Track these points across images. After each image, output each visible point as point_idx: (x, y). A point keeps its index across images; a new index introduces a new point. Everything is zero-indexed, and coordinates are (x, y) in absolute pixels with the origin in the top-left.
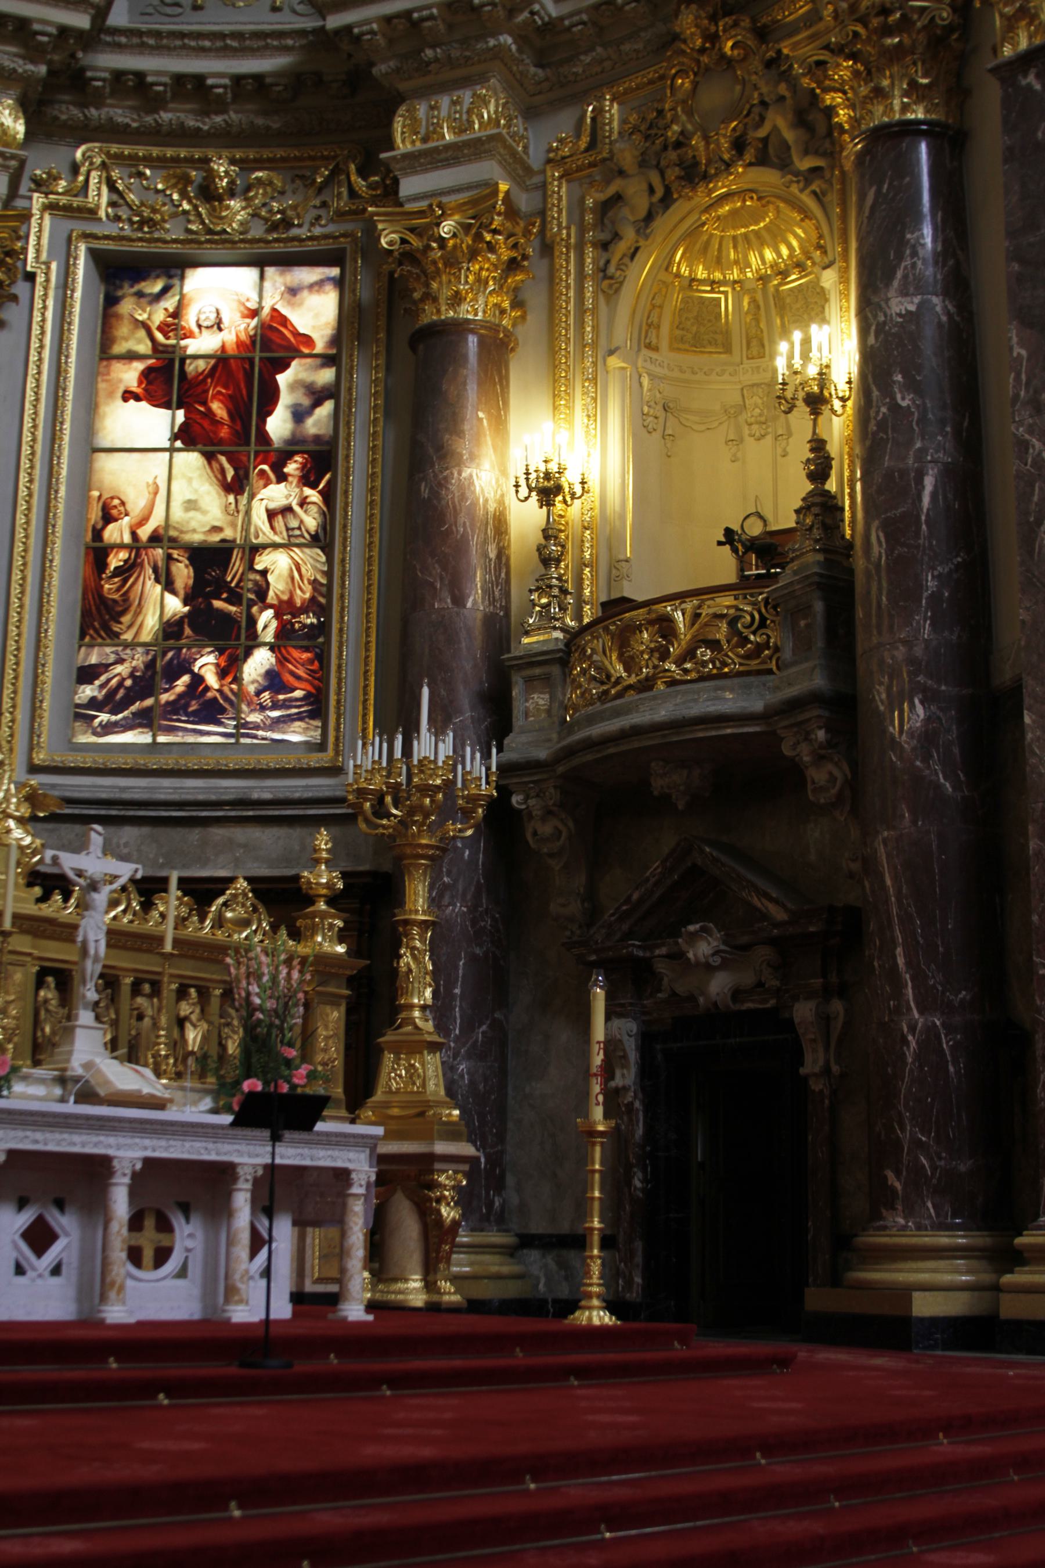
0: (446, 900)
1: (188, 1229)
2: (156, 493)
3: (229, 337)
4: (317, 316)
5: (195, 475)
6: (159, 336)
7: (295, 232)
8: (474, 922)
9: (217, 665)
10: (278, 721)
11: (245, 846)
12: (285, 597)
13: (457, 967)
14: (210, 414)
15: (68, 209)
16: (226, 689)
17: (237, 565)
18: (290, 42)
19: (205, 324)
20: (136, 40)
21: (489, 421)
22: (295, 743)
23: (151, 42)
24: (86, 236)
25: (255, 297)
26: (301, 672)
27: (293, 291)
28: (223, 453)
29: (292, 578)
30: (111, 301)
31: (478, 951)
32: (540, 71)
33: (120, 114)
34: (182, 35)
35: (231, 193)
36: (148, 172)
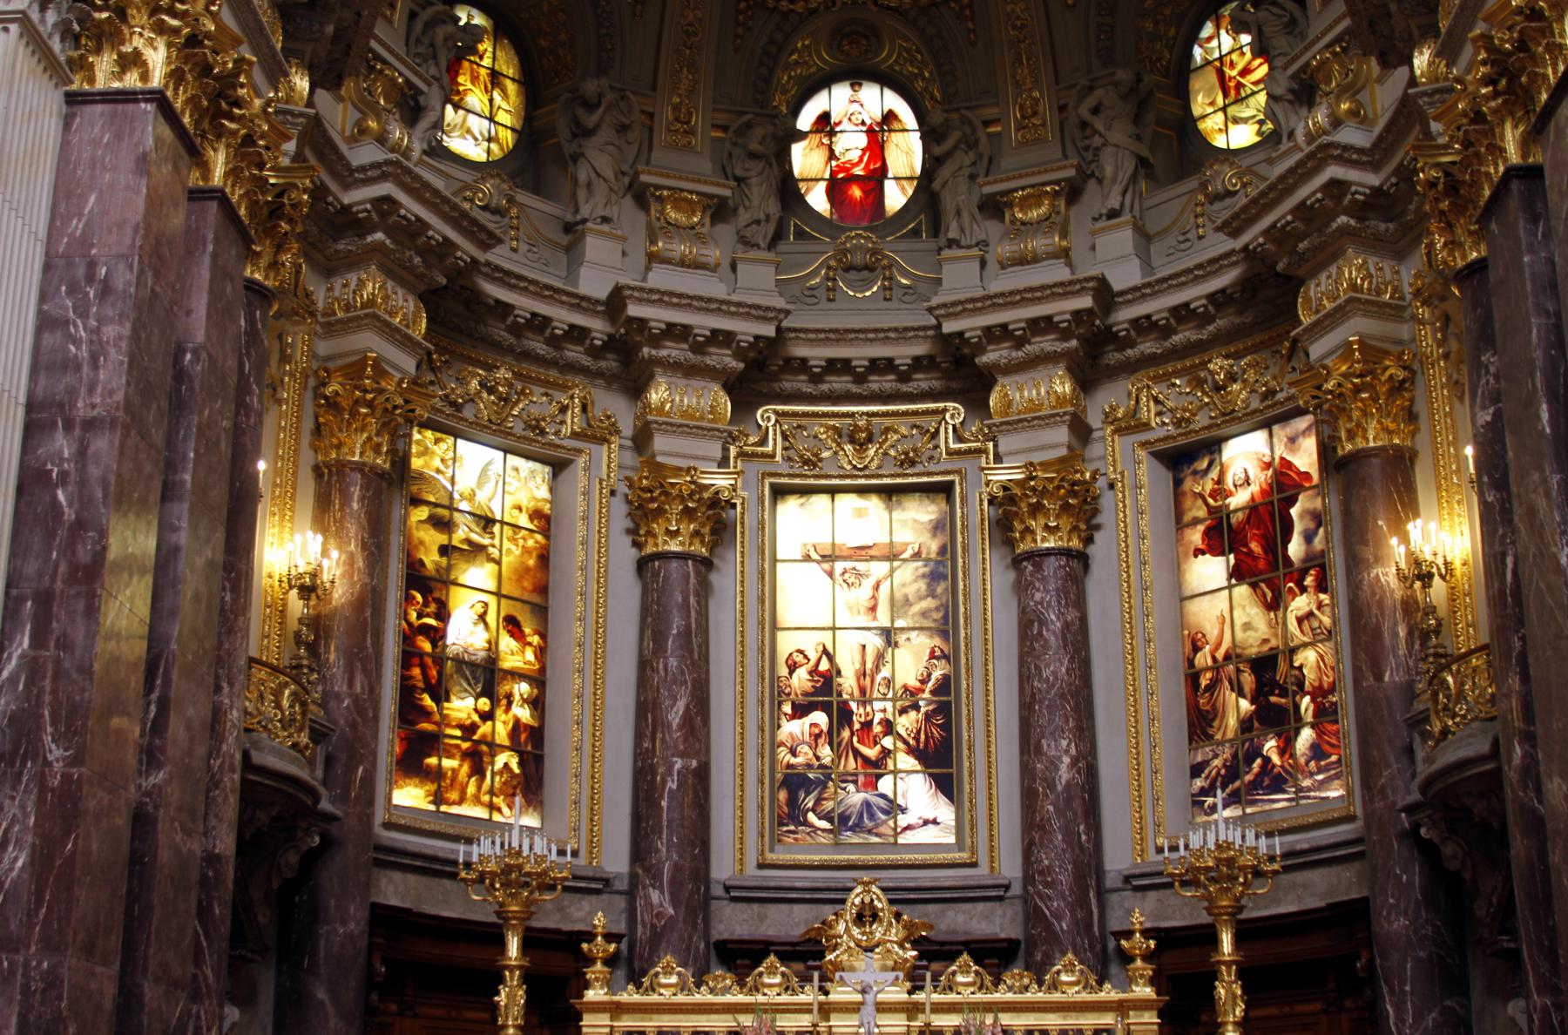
0: (1393, 917)
2: (1223, 623)
3: (1255, 488)
4: (1310, 455)
5: (1246, 602)
6: (1211, 501)
7: (1280, 396)
9: (1278, 747)
10: (1322, 782)
11: (1303, 886)
12: (1316, 684)
13: (1405, 969)
14: (1250, 549)
15: (1127, 428)
17: (1282, 666)
18: (1234, 259)
19: (1239, 483)
20: (1138, 294)
21: (1388, 527)
22: (1334, 798)
23: (1148, 291)
24: (1144, 444)
25: (1268, 452)
26: (1333, 741)
27: (1292, 440)
28: (1263, 581)
29: (1319, 667)
30: (1178, 483)
31: (1422, 954)
32: (1391, 225)
33: (1148, 347)
34: (1164, 280)
35: (1232, 378)
36: (1178, 382)
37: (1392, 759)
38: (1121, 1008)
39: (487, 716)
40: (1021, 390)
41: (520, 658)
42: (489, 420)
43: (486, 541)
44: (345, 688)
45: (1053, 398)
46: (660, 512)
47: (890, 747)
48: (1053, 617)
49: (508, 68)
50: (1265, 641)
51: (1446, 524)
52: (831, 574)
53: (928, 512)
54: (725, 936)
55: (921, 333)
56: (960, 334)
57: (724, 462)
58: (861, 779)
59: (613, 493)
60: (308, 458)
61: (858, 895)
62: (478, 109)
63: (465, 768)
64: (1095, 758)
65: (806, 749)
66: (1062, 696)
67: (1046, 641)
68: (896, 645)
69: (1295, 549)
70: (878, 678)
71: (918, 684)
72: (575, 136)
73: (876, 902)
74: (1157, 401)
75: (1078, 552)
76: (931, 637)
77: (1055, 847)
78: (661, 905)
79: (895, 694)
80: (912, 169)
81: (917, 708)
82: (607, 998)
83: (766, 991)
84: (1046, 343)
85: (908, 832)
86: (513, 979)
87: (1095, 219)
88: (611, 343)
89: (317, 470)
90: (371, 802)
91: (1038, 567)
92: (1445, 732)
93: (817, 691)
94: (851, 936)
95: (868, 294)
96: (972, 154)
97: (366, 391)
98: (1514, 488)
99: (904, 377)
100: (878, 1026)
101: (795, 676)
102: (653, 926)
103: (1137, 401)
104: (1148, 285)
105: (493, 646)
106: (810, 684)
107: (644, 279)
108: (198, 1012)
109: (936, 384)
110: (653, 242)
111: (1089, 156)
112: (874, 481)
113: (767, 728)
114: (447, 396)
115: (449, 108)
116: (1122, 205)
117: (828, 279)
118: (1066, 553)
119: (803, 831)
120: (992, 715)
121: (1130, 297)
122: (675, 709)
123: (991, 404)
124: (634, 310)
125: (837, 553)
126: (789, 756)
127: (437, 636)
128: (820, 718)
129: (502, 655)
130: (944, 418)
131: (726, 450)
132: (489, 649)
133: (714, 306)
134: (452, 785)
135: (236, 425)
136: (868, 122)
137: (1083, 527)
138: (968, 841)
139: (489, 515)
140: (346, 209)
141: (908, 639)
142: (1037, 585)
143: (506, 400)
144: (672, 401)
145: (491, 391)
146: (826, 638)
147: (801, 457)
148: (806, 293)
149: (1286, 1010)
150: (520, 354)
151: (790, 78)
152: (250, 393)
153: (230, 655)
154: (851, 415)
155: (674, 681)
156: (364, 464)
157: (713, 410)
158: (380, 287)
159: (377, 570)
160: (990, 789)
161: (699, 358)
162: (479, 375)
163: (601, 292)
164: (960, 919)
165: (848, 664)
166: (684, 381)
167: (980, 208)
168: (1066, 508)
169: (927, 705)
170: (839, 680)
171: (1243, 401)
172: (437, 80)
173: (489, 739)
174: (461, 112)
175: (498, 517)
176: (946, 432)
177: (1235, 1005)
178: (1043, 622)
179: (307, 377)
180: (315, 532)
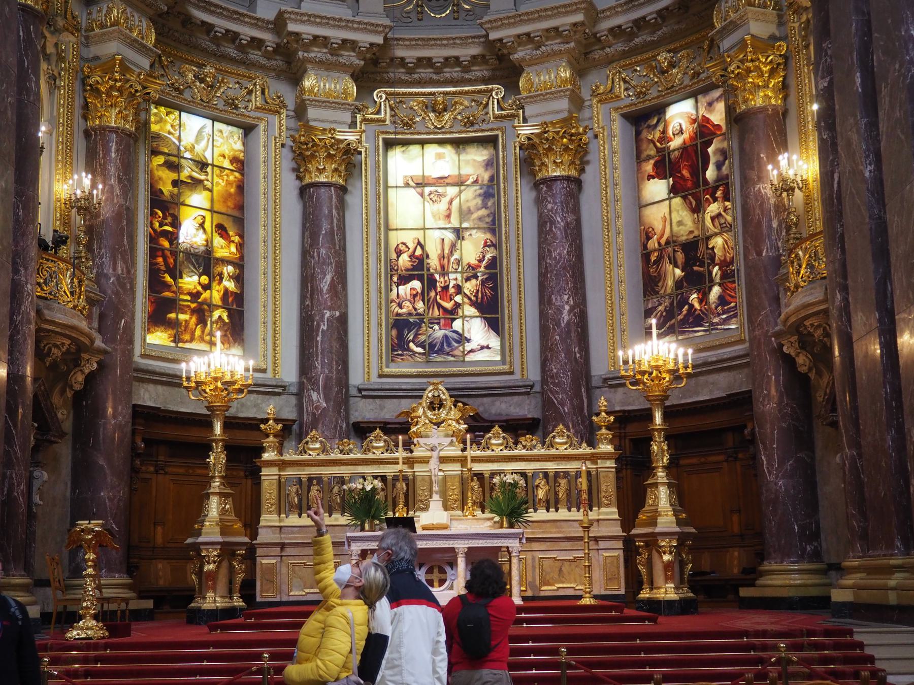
1: (453, 572)
3: (686, 136)
4: (721, 113)
6: (658, 144)
7: (703, 76)
8: (780, 411)
9: (698, 298)
11: (713, 383)
12: (722, 259)
14: (682, 175)
16: (703, 309)
17: (701, 248)
19: (677, 132)
24: (616, 109)
25: (694, 112)
26: (733, 294)
27: (710, 104)
29: (724, 248)
35: (672, 65)
36: (638, 69)
37: (766, 303)
38: (593, 458)
39: (207, 287)
40: (539, 75)
41: (227, 251)
42: (201, 100)
43: (203, 177)
44: (111, 270)
45: (559, 81)
46: (313, 156)
47: (460, 302)
48: (559, 219)
50: (691, 232)
51: (804, 155)
52: (422, 195)
53: (482, 155)
54: (359, 419)
55: (477, 40)
56: (501, 40)
57: (353, 125)
58: (442, 322)
59: (283, 145)
60: (79, 125)
61: (430, 391)
63: (194, 320)
64: (585, 306)
65: (408, 304)
66: (564, 268)
67: (555, 234)
68: (463, 238)
69: (711, 174)
70: (452, 259)
71: (477, 262)
73: (442, 396)
74: (625, 81)
75: (574, 178)
76: (485, 233)
77: (560, 361)
78: (318, 401)
79: (463, 269)
81: (476, 277)
82: (276, 458)
83: (374, 451)
84: (555, 45)
85: (471, 354)
86: (218, 448)
88: (278, 49)
89: (87, 134)
90: (131, 342)
91: (550, 188)
92: (797, 286)
93: (414, 268)
94: (426, 416)
95: (443, 15)
97: (116, 81)
98: (838, 129)
99: (466, 70)
100: (443, 471)
101: (401, 259)
102: (314, 414)
103: (613, 82)
105: (209, 244)
106: (410, 264)
107: (299, 7)
108: (12, 473)
109: (486, 73)
112: (448, 136)
113: (383, 291)
114: (173, 84)
117: (418, 6)
118: (567, 178)
119: (407, 354)
120: (522, 281)
122: (325, 280)
123: (520, 85)
124: (292, 27)
125: (426, 181)
126: (397, 308)
127: (173, 237)
128: (416, 284)
129: (215, 249)
130: (491, 95)
131: (354, 117)
132: (207, 245)
133: (343, 24)
134: (185, 330)
135: (20, 101)
137: (578, 162)
138: (508, 358)
139: (204, 160)
141: (471, 235)
142: (549, 199)
143: (212, 87)
144: (319, 86)
145: (202, 81)
146: (419, 235)
147: (402, 121)
148: (404, 15)
149: (703, 460)
150: (219, 56)
152: (30, 81)
153: (24, 251)
154: (433, 94)
155: (324, 263)
156: (118, 128)
157: (345, 91)
158: (122, 12)
159: (130, 195)
160: (521, 326)
161: (335, 58)
162: (194, 71)
163: (271, 15)
164: (503, 406)
165: (433, 251)
166: (326, 73)
168: (567, 149)
169: (483, 275)
170: (429, 261)
171: (679, 80)
173: (209, 301)
175: (210, 162)
176: (493, 104)
177: (663, 456)
178: (553, 223)
179: (77, 72)
180: (87, 173)
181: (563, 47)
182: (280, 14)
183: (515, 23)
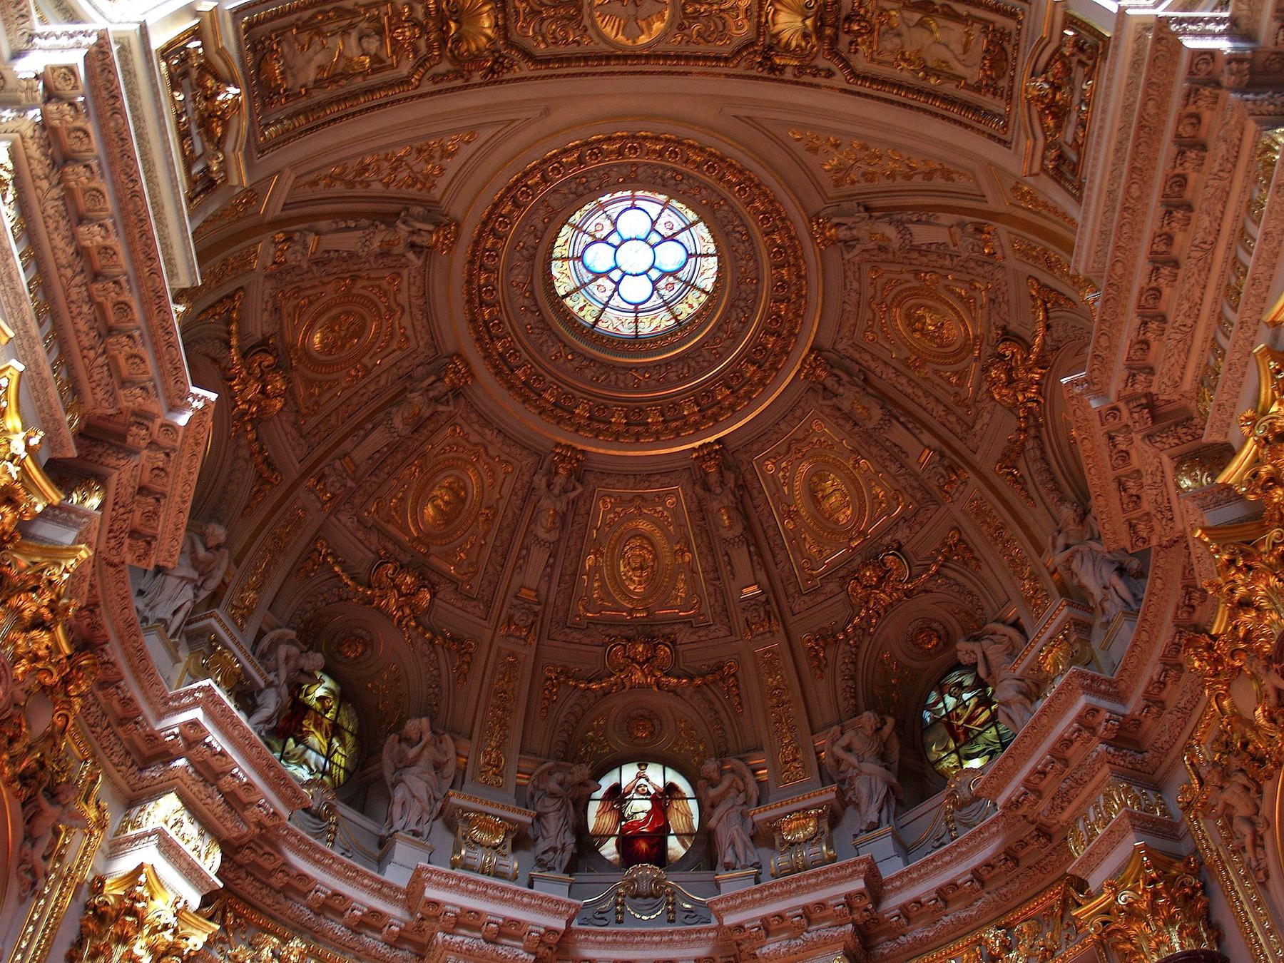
18: (994, 829)
33: (919, 931)
49: (349, 725)
56: (740, 927)
62: (317, 746)
72: (397, 769)
80: (691, 826)
87: (855, 836)
96: (742, 795)
104: (917, 869)
110: (457, 851)
111: (845, 787)
115: (291, 740)
116: (879, 819)
121: (898, 883)
124: (431, 893)
136: (652, 791)
140: (152, 737)
151: (587, 753)
161: (491, 947)
167: (752, 838)
172: (277, 686)
174: (301, 747)
181: (836, 932)
182: (418, 872)
183: (761, 899)
